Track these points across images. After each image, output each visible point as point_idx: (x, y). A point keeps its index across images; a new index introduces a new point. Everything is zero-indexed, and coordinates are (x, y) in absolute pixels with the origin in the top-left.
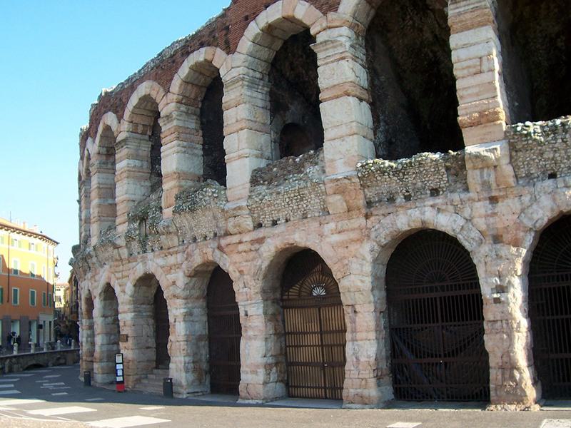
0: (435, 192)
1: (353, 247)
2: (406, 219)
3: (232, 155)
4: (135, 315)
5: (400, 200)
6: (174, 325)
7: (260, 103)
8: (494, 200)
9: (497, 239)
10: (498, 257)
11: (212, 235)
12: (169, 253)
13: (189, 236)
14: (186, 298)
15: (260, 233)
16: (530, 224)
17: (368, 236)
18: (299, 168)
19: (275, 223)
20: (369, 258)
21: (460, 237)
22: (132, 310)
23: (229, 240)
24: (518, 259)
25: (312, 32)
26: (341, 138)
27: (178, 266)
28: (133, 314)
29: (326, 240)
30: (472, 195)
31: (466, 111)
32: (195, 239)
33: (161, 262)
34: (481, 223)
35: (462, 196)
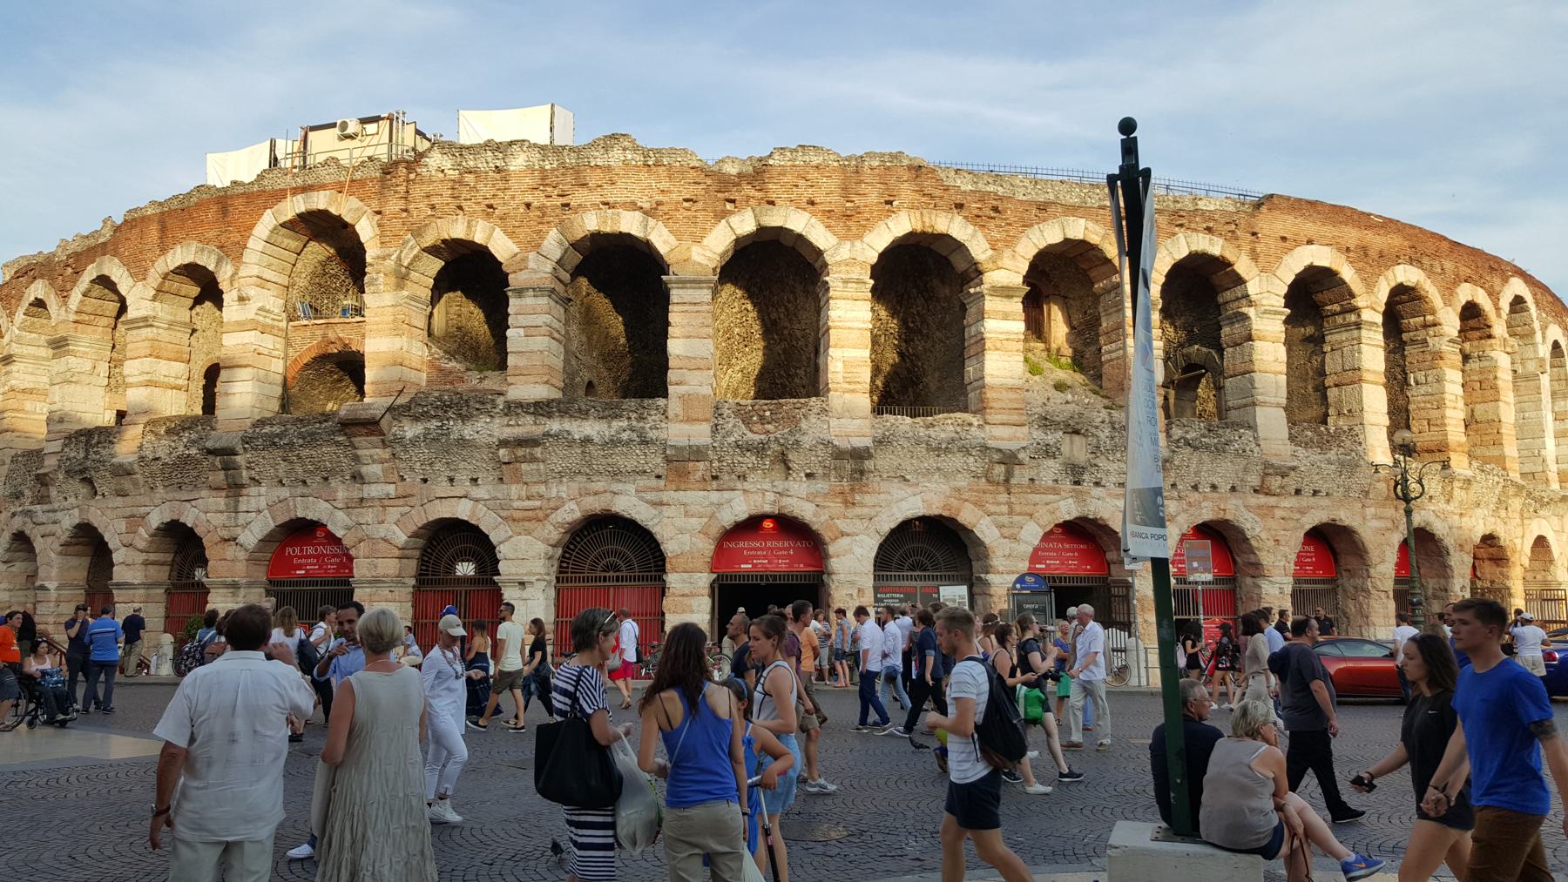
1: (1388, 534)
13: (1192, 480)
15: (1305, 500)
19: (1315, 493)
23: (1262, 499)
32: (1195, 488)
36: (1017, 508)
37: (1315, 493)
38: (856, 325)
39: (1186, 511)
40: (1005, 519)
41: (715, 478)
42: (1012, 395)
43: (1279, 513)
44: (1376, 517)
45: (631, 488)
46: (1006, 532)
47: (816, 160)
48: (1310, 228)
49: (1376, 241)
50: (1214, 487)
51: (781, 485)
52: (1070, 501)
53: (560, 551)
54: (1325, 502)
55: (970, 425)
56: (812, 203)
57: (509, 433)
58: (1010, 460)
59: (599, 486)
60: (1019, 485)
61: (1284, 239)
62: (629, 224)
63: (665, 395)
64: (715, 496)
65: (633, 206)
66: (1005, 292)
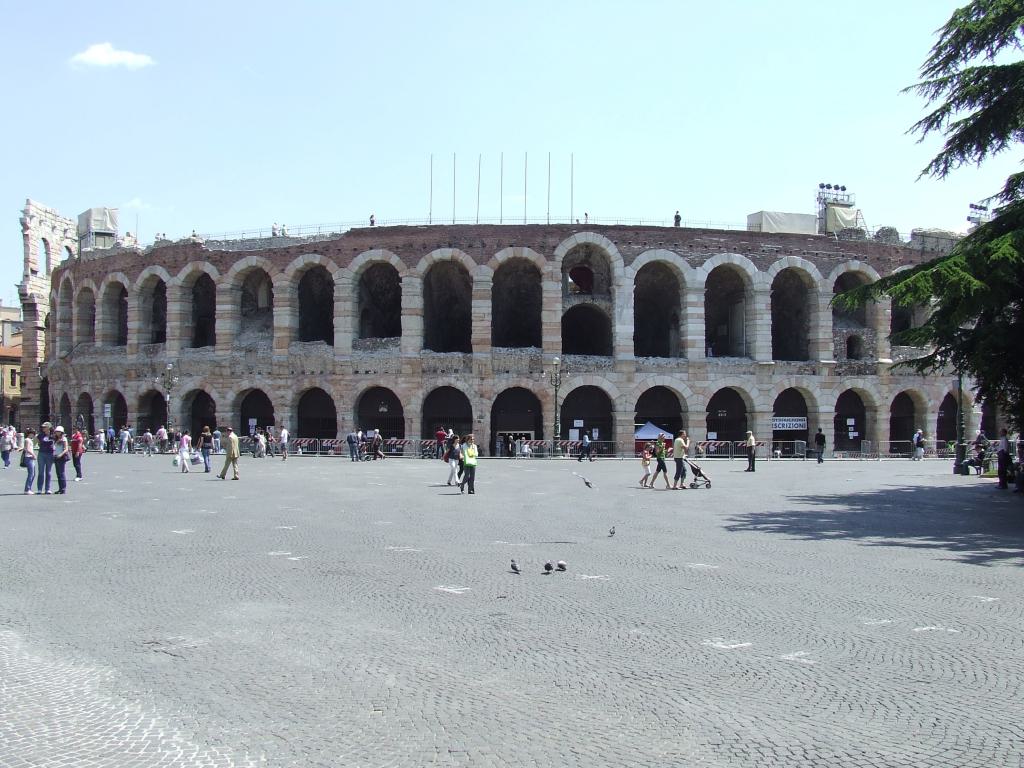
0: (456, 371)
2: (441, 382)
5: (439, 371)
7: (356, 300)
8: (482, 379)
9: (482, 396)
10: (482, 403)
13: (299, 370)
15: (358, 376)
16: (496, 390)
17: (422, 387)
18: (385, 346)
19: (367, 372)
20: (421, 397)
21: (466, 393)
23: (334, 376)
24: (488, 404)
25: (400, 275)
26: (412, 336)
27: (289, 387)
29: (399, 387)
30: (474, 375)
31: (475, 336)
32: (303, 373)
34: (476, 388)
35: (471, 375)
37: (367, 372)
42: (226, 337)
43: (343, 383)
44: (403, 382)
47: (165, 245)
48: (369, 241)
49: (419, 240)
50: (313, 373)
54: (373, 376)
56: (165, 262)
57: (93, 361)
58: (219, 365)
59: (111, 380)
61: (355, 249)
62: (121, 277)
63: (126, 344)
65: (123, 271)
66: (224, 291)
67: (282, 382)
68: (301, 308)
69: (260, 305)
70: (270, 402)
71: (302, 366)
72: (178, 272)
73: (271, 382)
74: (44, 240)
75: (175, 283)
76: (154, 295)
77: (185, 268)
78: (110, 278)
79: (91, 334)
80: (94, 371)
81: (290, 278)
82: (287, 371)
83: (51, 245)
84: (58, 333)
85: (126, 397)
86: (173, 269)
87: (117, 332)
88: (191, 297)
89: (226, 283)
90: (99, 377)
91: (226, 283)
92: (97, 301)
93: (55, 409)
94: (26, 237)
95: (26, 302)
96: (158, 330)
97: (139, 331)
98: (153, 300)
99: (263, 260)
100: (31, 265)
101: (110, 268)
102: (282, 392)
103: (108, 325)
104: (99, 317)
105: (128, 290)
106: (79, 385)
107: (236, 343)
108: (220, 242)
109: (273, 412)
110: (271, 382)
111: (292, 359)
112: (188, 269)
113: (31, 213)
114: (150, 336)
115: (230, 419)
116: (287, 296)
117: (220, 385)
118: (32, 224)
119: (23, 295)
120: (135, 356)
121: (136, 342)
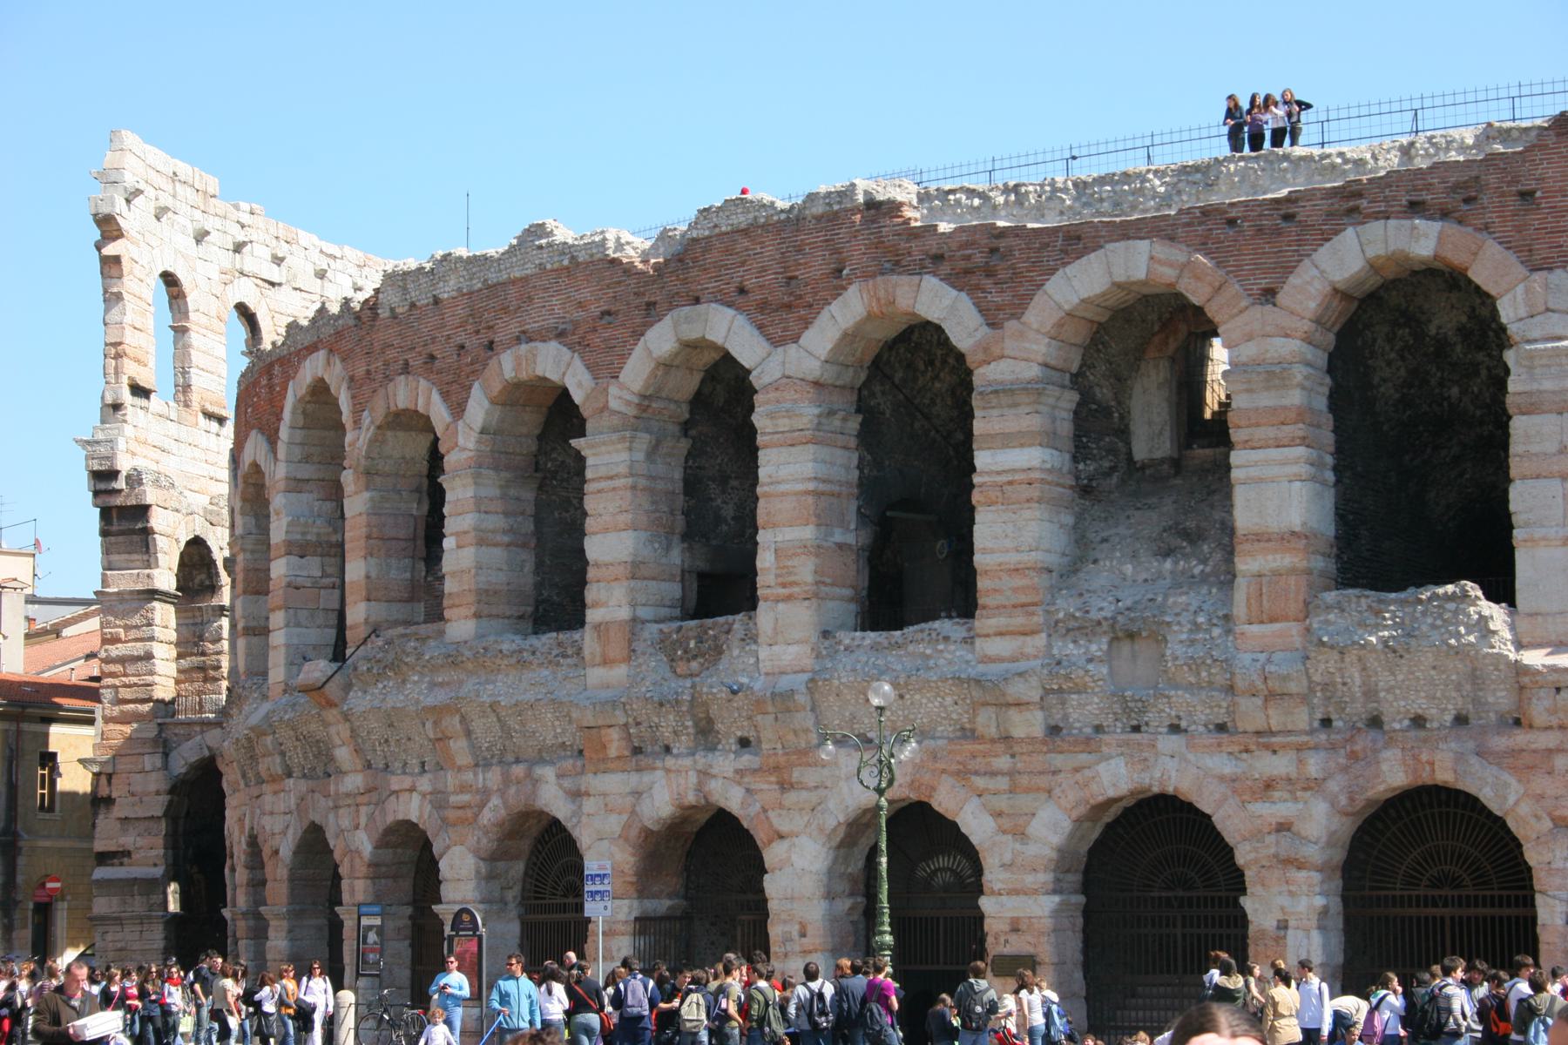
3: (1538, 533)
4: (1061, 904)
6: (1280, 940)
11: (1448, 718)
12: (1267, 747)
13: (1358, 709)
14: (1320, 870)
22: (1051, 886)
23: (1520, 738)
27: (1313, 786)
28: (1057, 898)
32: (1375, 722)
33: (1223, 764)
36: (1024, 780)
38: (783, 488)
39: (1345, 769)
40: (1002, 803)
41: (637, 751)
42: (1019, 582)
45: (548, 772)
46: (1006, 823)
47: (741, 220)
50: (1418, 721)
51: (701, 759)
52: (1121, 761)
53: (519, 868)
55: (946, 639)
56: (742, 291)
57: (440, 697)
59: (518, 770)
60: (1032, 740)
63: (578, 621)
64: (634, 779)
67: (1279, 765)
68: (1339, 451)
69: (1140, 452)
70: (1227, 852)
71: (1370, 693)
72: (806, 323)
73: (1228, 767)
74: (169, 279)
75: (795, 371)
76: (686, 427)
77: (835, 307)
78: (508, 366)
79: (424, 593)
80: (442, 739)
81: (1307, 326)
82: (1302, 718)
83: (192, 299)
84: (277, 594)
85: (584, 838)
86: (783, 314)
87: (528, 580)
88: (854, 424)
89: (1016, 362)
90: (464, 759)
91: (1016, 362)
92: (450, 461)
93: (259, 892)
94: (111, 266)
95: (118, 501)
96: (701, 565)
97: (636, 570)
98: (684, 445)
99: (1177, 254)
100: (131, 369)
101: (507, 328)
102: (1278, 809)
103: (497, 555)
104: (459, 520)
105: (585, 412)
106: (375, 793)
107: (1066, 605)
108: (983, 196)
109: (1243, 890)
110: (1228, 767)
111: (1324, 665)
112: (846, 312)
113: (130, 180)
114: (674, 590)
115: (1048, 923)
116: (1295, 398)
117: (1002, 783)
118: (132, 219)
119: (103, 478)
120: (620, 672)
121: (624, 613)
